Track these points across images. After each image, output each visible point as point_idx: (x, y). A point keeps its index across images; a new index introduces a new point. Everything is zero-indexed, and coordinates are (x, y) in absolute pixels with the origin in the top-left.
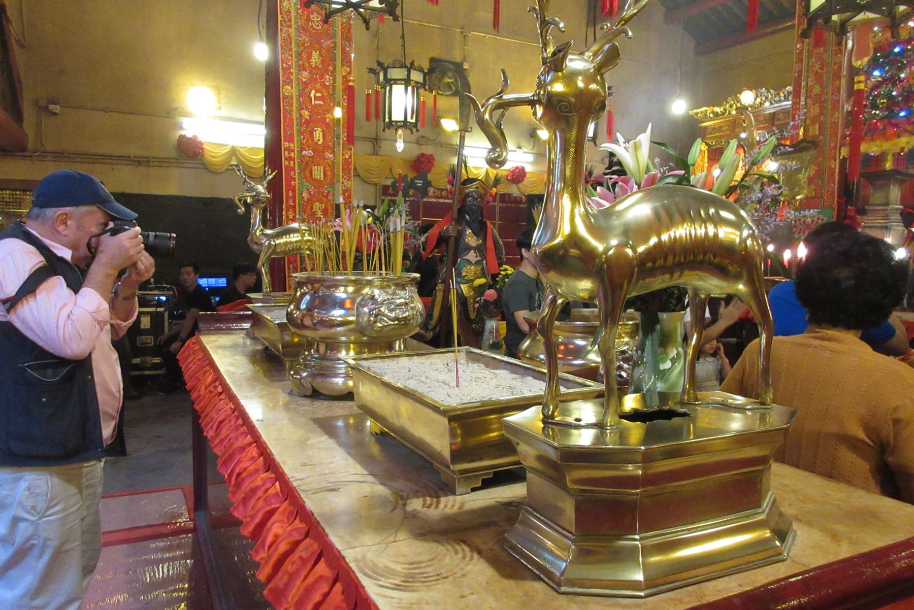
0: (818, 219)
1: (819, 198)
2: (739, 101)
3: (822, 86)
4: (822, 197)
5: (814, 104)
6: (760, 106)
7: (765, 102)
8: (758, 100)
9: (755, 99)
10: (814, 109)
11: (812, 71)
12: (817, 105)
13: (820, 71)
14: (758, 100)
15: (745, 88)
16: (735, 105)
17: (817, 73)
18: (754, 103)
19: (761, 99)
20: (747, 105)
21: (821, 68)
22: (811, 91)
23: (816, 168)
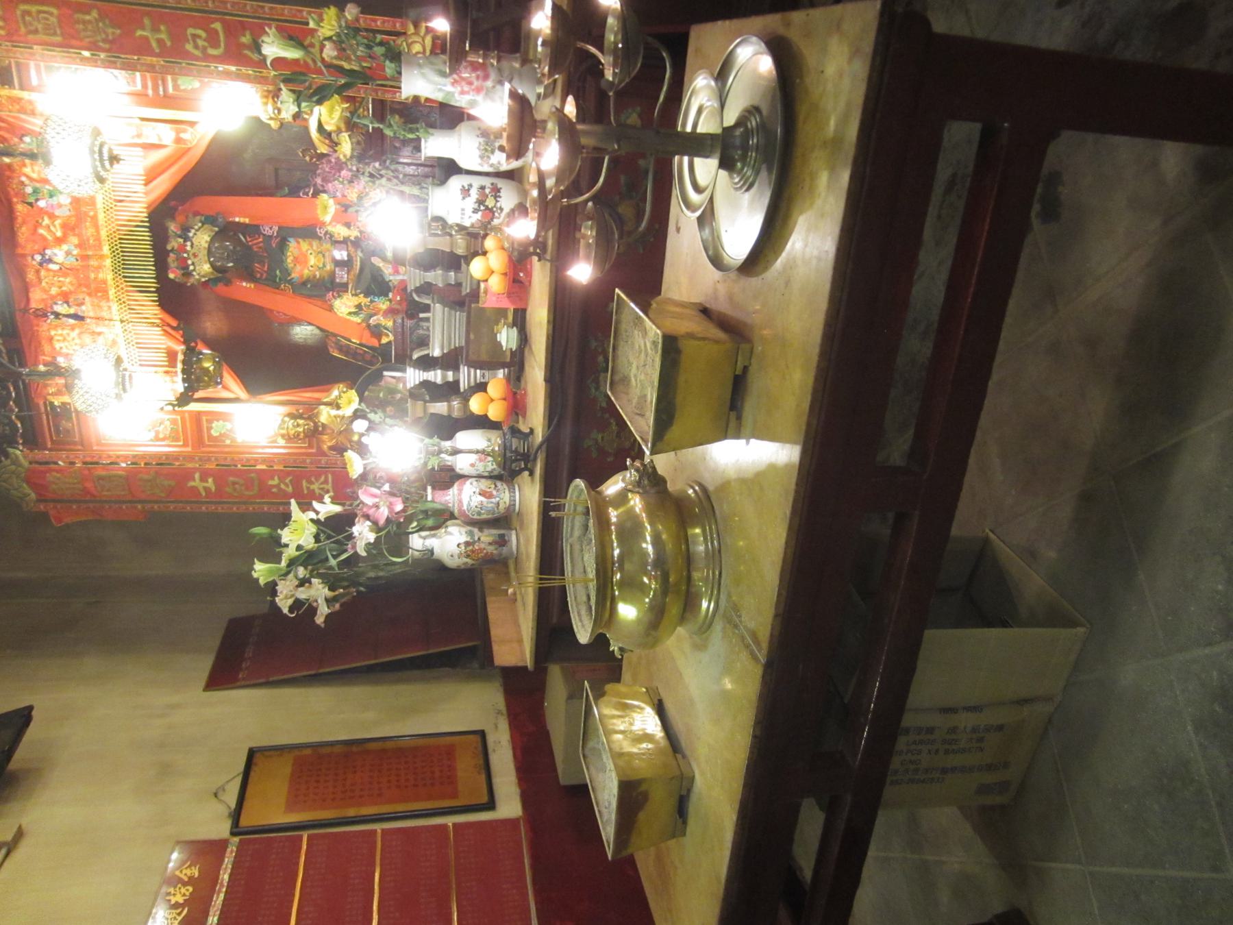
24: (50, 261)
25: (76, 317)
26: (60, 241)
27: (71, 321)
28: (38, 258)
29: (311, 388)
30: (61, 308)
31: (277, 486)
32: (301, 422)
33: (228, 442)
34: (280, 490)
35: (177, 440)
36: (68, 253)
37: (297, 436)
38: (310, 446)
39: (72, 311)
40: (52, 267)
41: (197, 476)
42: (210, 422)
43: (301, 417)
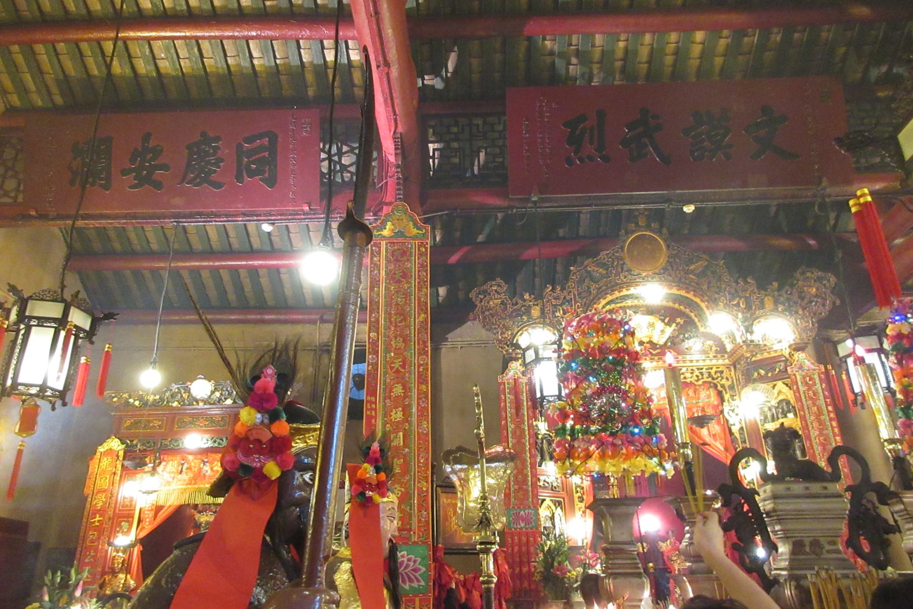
0: (409, 560)
1: (406, 530)
2: (188, 390)
3: (404, 387)
4: (410, 530)
5: (396, 408)
6: (219, 402)
7: (226, 399)
8: (218, 394)
9: (213, 392)
10: (396, 413)
11: (392, 368)
12: (400, 409)
13: (400, 369)
14: (218, 394)
15: (200, 376)
16: (179, 395)
17: (397, 371)
18: (210, 397)
19: (221, 394)
20: (198, 397)
21: (403, 366)
22: (391, 391)
23: (403, 490)
24: (204, 464)
25: (181, 472)
26: (212, 469)
27: (180, 469)
28: (206, 460)
29: (140, 567)
30: (185, 466)
31: (89, 555)
32: (120, 566)
33: (118, 529)
34: (87, 556)
35: (123, 507)
36: (207, 471)
37: (113, 563)
38: (109, 568)
39: (184, 470)
40: (202, 465)
41: (101, 519)
42: (128, 522)
43: (123, 565)
